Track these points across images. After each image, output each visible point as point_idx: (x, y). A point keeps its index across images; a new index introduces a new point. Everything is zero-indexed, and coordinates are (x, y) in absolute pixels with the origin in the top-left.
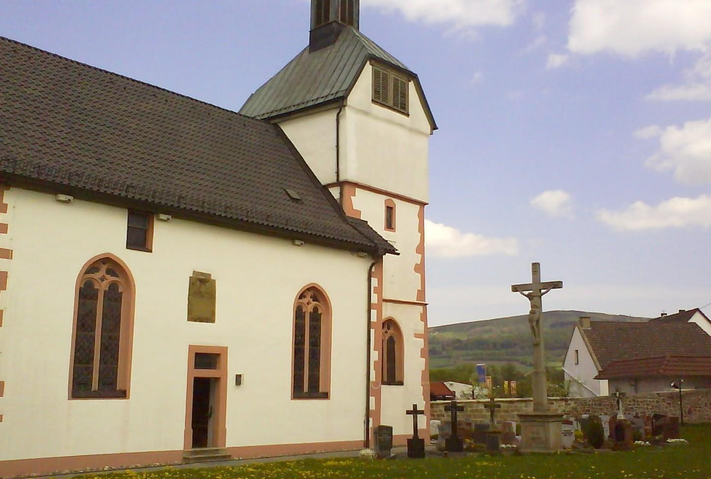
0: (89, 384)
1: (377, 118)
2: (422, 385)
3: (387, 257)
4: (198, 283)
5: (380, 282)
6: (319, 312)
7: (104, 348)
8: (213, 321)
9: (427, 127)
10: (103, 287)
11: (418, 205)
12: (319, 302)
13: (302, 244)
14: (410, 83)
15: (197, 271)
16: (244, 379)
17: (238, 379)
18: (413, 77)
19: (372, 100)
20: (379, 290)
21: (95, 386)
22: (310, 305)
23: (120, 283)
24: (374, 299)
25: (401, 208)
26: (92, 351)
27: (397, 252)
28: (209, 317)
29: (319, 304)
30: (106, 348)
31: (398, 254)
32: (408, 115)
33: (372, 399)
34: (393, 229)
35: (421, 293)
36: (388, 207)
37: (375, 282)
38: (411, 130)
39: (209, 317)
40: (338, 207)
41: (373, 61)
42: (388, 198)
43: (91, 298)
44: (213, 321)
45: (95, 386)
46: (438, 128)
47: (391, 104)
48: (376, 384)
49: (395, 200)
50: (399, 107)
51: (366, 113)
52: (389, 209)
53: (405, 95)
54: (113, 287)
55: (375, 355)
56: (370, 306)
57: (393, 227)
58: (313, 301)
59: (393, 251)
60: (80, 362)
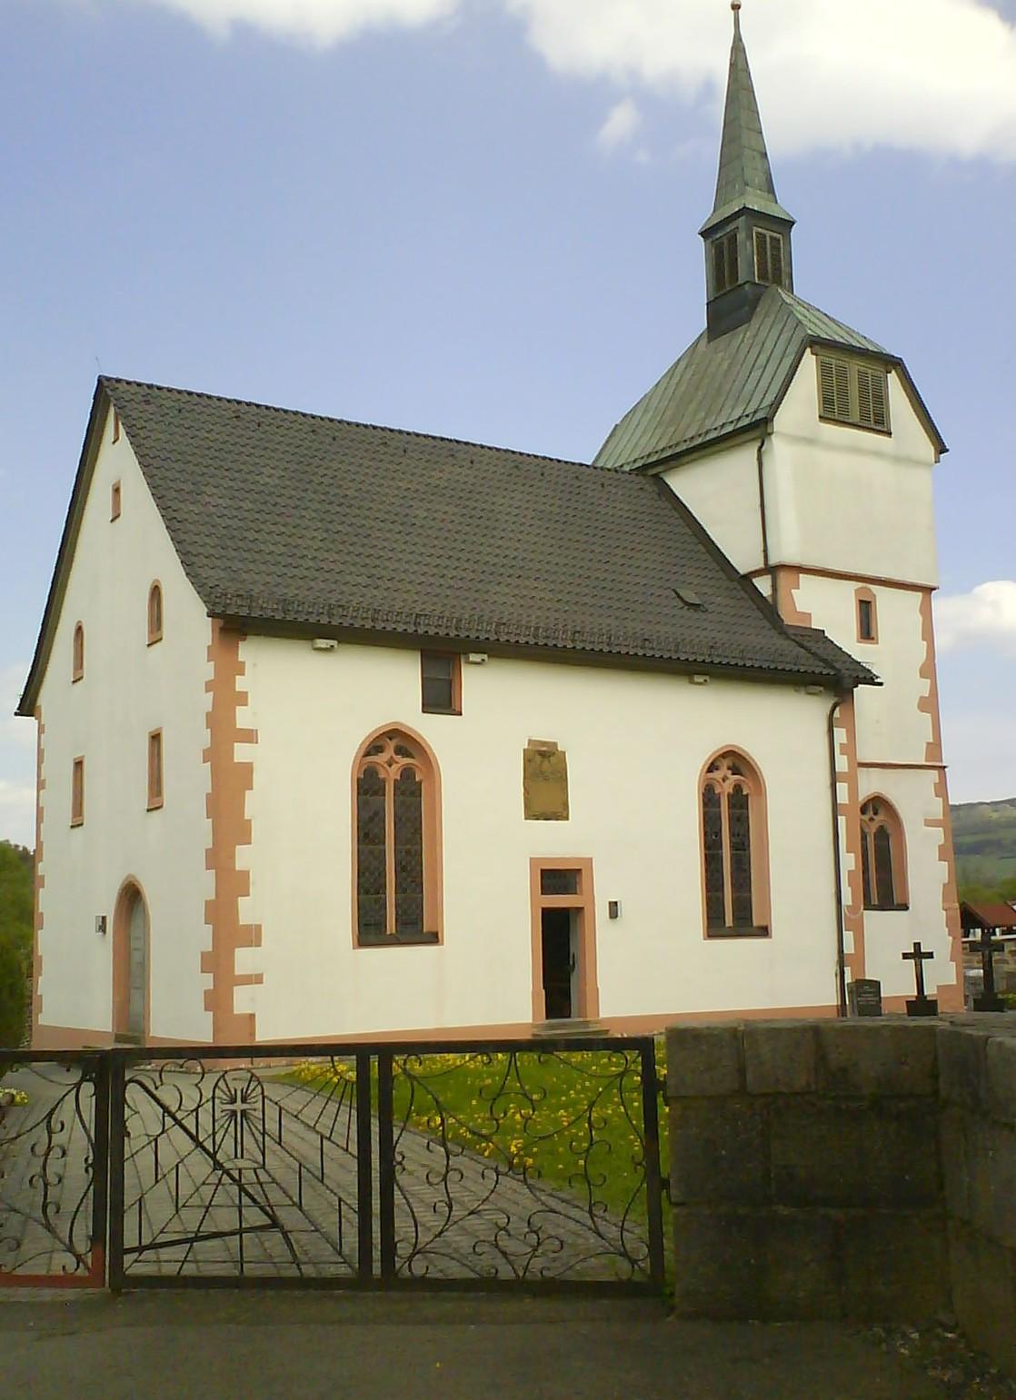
0: (381, 925)
1: (830, 447)
2: (943, 909)
3: (861, 691)
4: (538, 758)
5: (852, 734)
6: (745, 793)
7: (401, 868)
8: (567, 818)
9: (929, 450)
10: (391, 774)
11: (919, 591)
12: (741, 775)
13: (706, 681)
14: (889, 375)
15: (533, 738)
16: (622, 909)
17: (614, 909)
18: (895, 363)
19: (820, 417)
20: (850, 749)
21: (391, 926)
22: (728, 782)
23: (417, 767)
24: (842, 764)
25: (885, 600)
26: (383, 874)
27: (878, 680)
28: (560, 813)
29: (742, 778)
30: (404, 869)
31: (881, 684)
32: (889, 434)
33: (848, 937)
34: (873, 639)
35: (935, 748)
36: (861, 601)
37: (840, 735)
38: (898, 460)
39: (560, 813)
40: (769, 610)
41: (817, 348)
42: (860, 585)
43: (375, 793)
44: (567, 818)
45: (391, 926)
46: (947, 450)
47: (856, 418)
48: (853, 909)
49: (874, 588)
50: (872, 422)
51: (810, 441)
52: (864, 605)
53: (881, 399)
54: (407, 773)
55: (850, 862)
56: (834, 778)
57: (873, 635)
58: (733, 774)
59: (871, 680)
60: (367, 892)
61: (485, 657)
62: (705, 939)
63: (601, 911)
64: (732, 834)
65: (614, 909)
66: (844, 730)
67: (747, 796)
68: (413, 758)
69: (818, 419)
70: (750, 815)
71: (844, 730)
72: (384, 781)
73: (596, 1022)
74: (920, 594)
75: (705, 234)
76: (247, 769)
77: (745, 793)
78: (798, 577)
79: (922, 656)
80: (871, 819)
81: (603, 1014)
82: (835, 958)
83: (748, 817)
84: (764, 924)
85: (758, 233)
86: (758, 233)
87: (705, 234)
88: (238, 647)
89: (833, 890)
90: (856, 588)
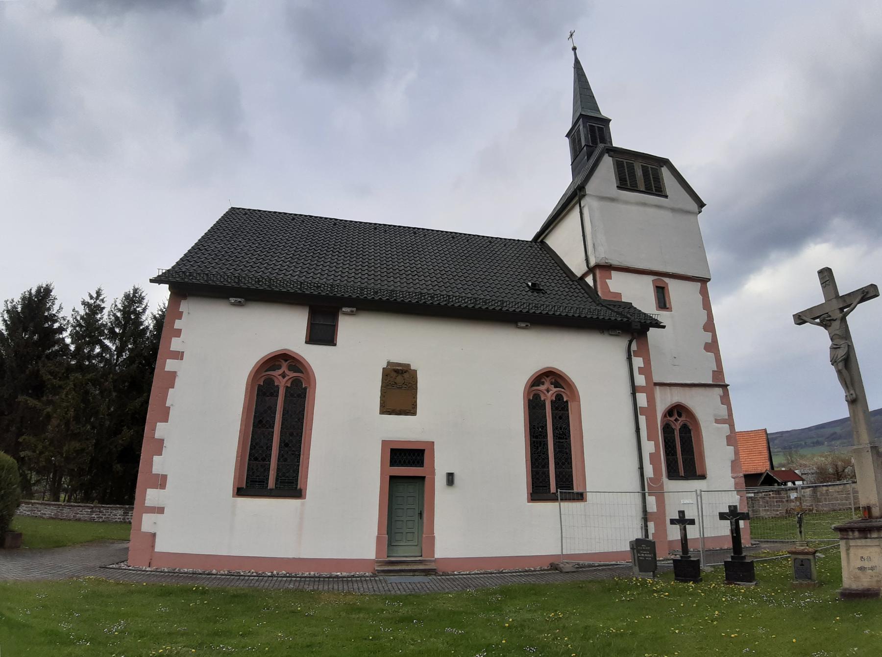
0: (264, 481)
1: (626, 202)
2: (732, 478)
3: (652, 332)
4: (394, 374)
5: (647, 362)
6: (565, 400)
7: (284, 444)
8: (414, 414)
9: (694, 206)
10: (282, 384)
11: (698, 282)
12: (563, 388)
13: (527, 326)
14: (662, 168)
15: (391, 361)
16: (457, 480)
17: (450, 479)
18: (665, 162)
19: (617, 187)
20: (646, 371)
21: (271, 483)
22: (551, 392)
23: (303, 378)
24: (640, 380)
25: (675, 288)
26: (270, 448)
27: (662, 324)
28: (410, 409)
29: (563, 390)
30: (287, 445)
31: (664, 327)
32: (666, 197)
33: (651, 500)
34: (668, 308)
35: (719, 372)
36: (658, 287)
37: (638, 362)
38: (673, 210)
39: (410, 409)
40: (592, 293)
41: (612, 153)
42: (656, 277)
43: (272, 395)
44: (414, 414)
45: (271, 483)
46: (706, 205)
47: (643, 189)
48: (657, 479)
49: (667, 280)
50: (654, 190)
51: (612, 200)
52: (661, 290)
53: (658, 179)
55: (649, 447)
56: (634, 390)
57: (668, 306)
58: (555, 387)
60: (256, 459)
61: (354, 309)
62: (528, 502)
63: (440, 480)
64: (555, 428)
65: (450, 479)
66: (642, 358)
67: (567, 402)
68: (303, 373)
69: (616, 188)
70: (570, 415)
71: (642, 358)
72: (278, 386)
73: (431, 561)
74: (699, 284)
75: (567, 136)
76: (173, 375)
77: (565, 400)
78: (611, 273)
79: (705, 318)
80: (676, 420)
81: (439, 554)
82: (640, 514)
83: (568, 416)
84: (580, 491)
85: (589, 125)
86: (589, 125)
87: (567, 136)
88: (180, 304)
89: (636, 465)
90: (653, 279)
